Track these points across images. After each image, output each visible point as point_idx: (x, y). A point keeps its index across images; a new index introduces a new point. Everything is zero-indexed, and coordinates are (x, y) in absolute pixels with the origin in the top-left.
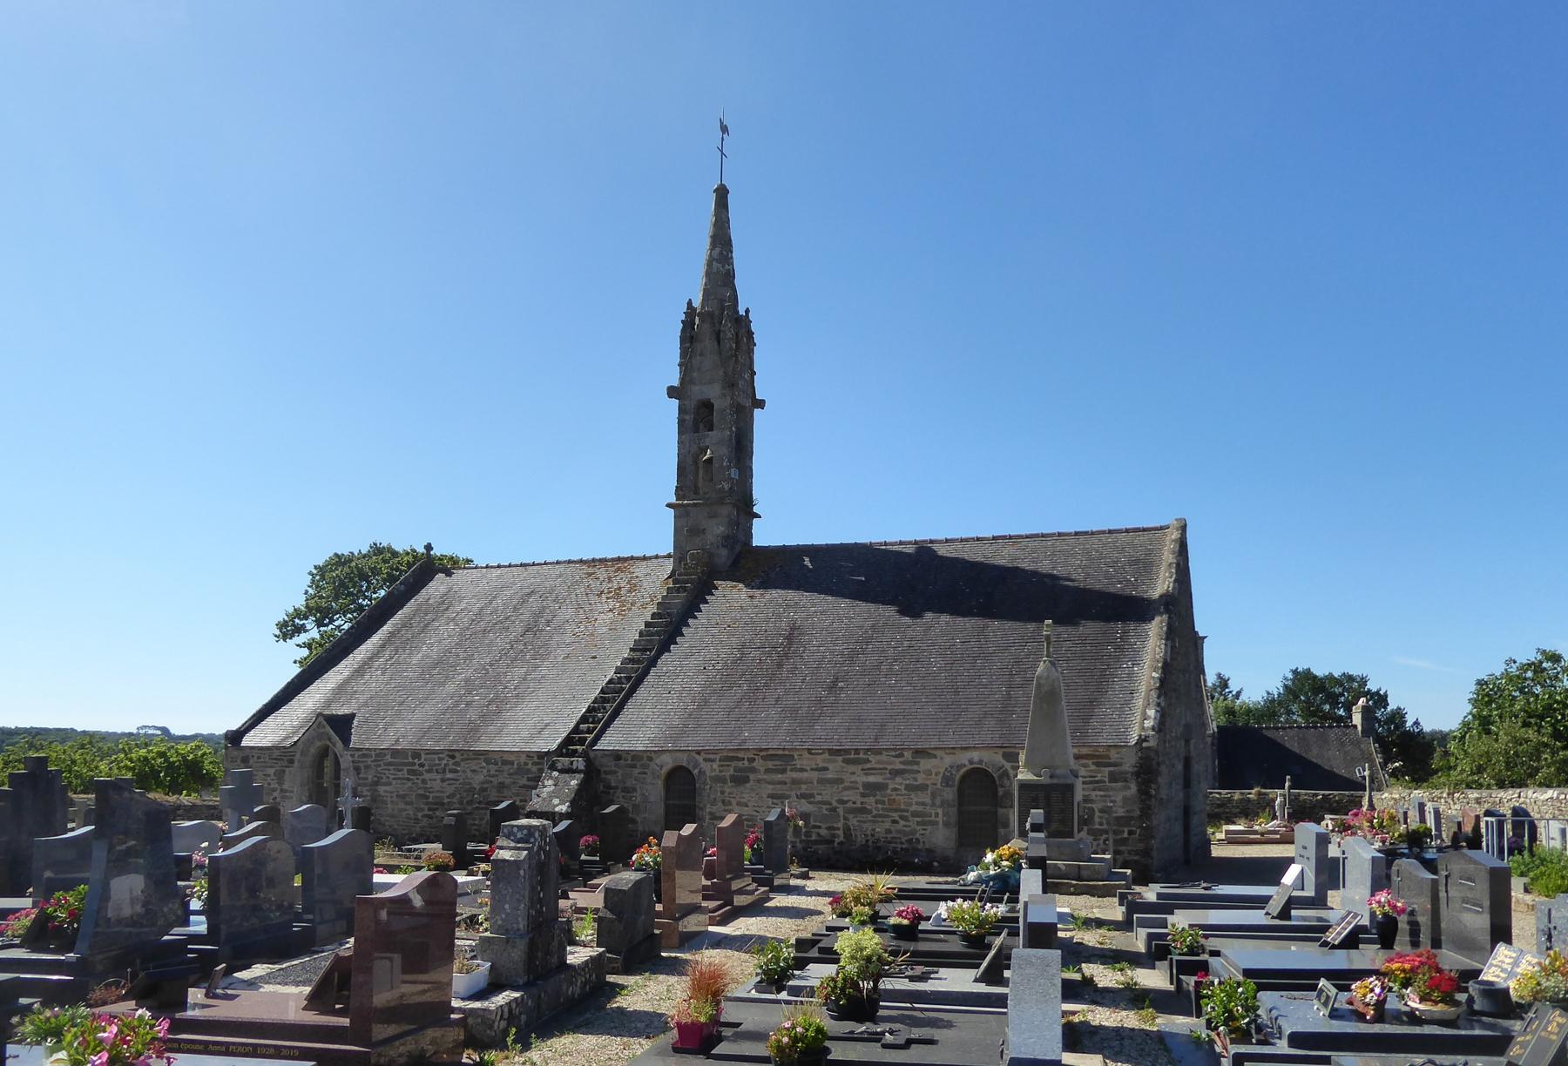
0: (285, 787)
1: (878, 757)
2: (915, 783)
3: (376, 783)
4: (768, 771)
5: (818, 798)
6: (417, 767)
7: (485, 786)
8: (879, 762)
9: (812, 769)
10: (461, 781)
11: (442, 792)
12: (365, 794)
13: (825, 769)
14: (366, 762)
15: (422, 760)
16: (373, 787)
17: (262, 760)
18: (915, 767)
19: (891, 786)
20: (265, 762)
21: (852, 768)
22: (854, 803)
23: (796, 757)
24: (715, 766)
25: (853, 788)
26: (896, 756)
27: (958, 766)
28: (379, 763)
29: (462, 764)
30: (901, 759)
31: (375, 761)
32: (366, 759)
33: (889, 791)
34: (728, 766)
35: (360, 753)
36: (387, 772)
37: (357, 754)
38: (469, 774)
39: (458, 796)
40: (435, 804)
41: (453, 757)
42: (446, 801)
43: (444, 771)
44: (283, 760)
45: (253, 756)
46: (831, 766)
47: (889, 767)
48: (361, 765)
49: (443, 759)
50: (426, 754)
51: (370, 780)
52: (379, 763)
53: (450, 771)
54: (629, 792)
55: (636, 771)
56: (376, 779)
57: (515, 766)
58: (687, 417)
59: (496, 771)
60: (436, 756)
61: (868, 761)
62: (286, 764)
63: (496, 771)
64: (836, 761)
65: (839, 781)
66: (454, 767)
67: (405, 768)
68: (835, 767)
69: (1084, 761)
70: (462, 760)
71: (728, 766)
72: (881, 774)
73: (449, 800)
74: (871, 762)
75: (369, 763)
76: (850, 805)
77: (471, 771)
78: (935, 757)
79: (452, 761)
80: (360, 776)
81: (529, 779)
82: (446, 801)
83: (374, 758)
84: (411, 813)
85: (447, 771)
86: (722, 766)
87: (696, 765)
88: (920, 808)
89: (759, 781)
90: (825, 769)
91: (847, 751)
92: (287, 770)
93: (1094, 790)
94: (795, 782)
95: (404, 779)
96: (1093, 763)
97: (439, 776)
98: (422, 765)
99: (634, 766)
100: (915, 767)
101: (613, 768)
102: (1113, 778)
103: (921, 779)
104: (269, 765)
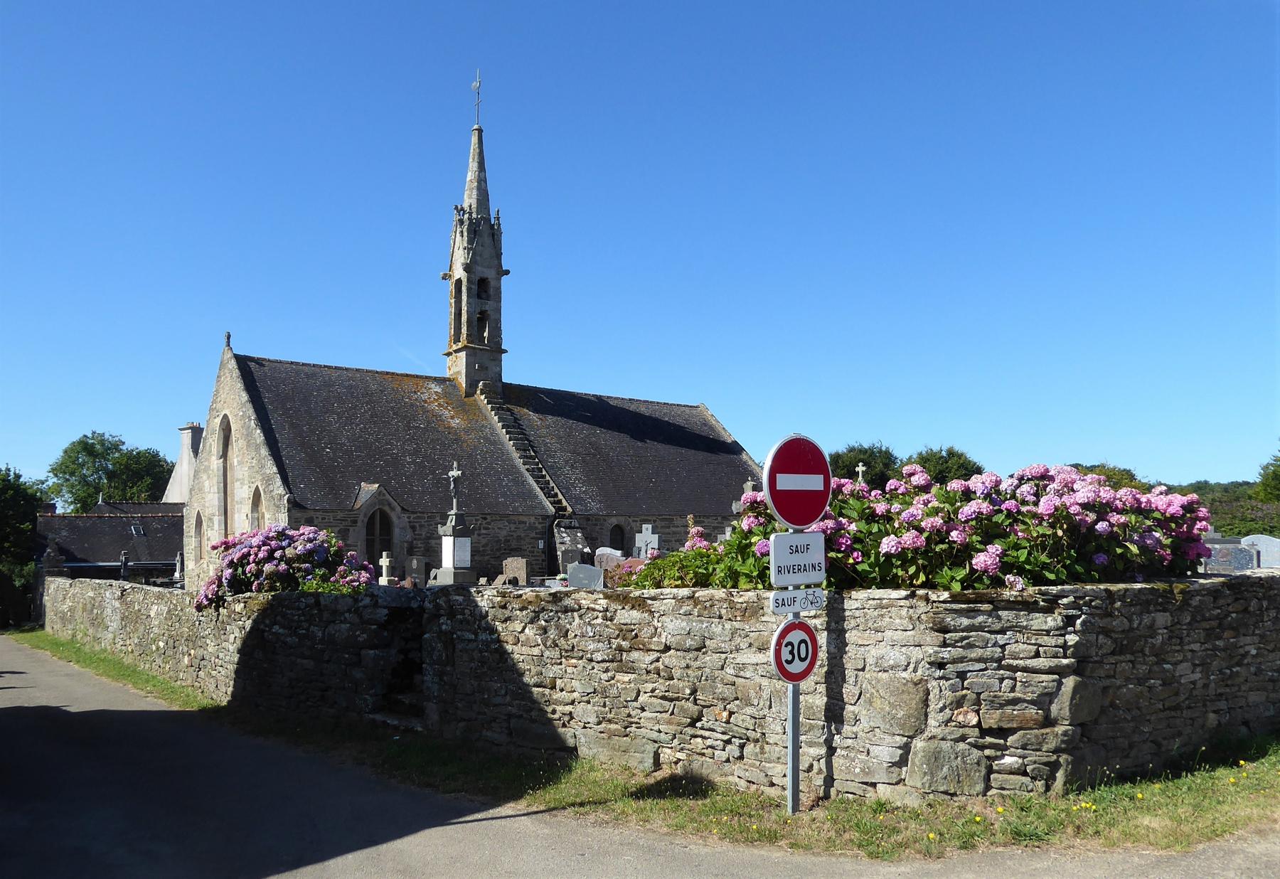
0: (349, 542)
3: (429, 538)
4: (662, 527)
7: (508, 538)
8: (708, 523)
11: (479, 543)
12: (420, 545)
17: (326, 520)
19: (713, 535)
20: (329, 522)
26: (715, 520)
29: (492, 523)
31: (427, 521)
37: (412, 516)
38: (497, 531)
39: (490, 545)
41: (485, 519)
42: (481, 549)
44: (347, 520)
45: (317, 518)
48: (417, 525)
51: (424, 536)
55: (598, 527)
56: (429, 535)
57: (527, 524)
58: (473, 287)
59: (516, 528)
61: (704, 522)
62: (350, 524)
63: (516, 528)
66: (486, 526)
70: (492, 521)
75: (423, 523)
77: (498, 528)
80: (416, 533)
81: (536, 534)
82: (481, 549)
87: (629, 524)
92: (351, 529)
94: (674, 533)
104: (334, 525)
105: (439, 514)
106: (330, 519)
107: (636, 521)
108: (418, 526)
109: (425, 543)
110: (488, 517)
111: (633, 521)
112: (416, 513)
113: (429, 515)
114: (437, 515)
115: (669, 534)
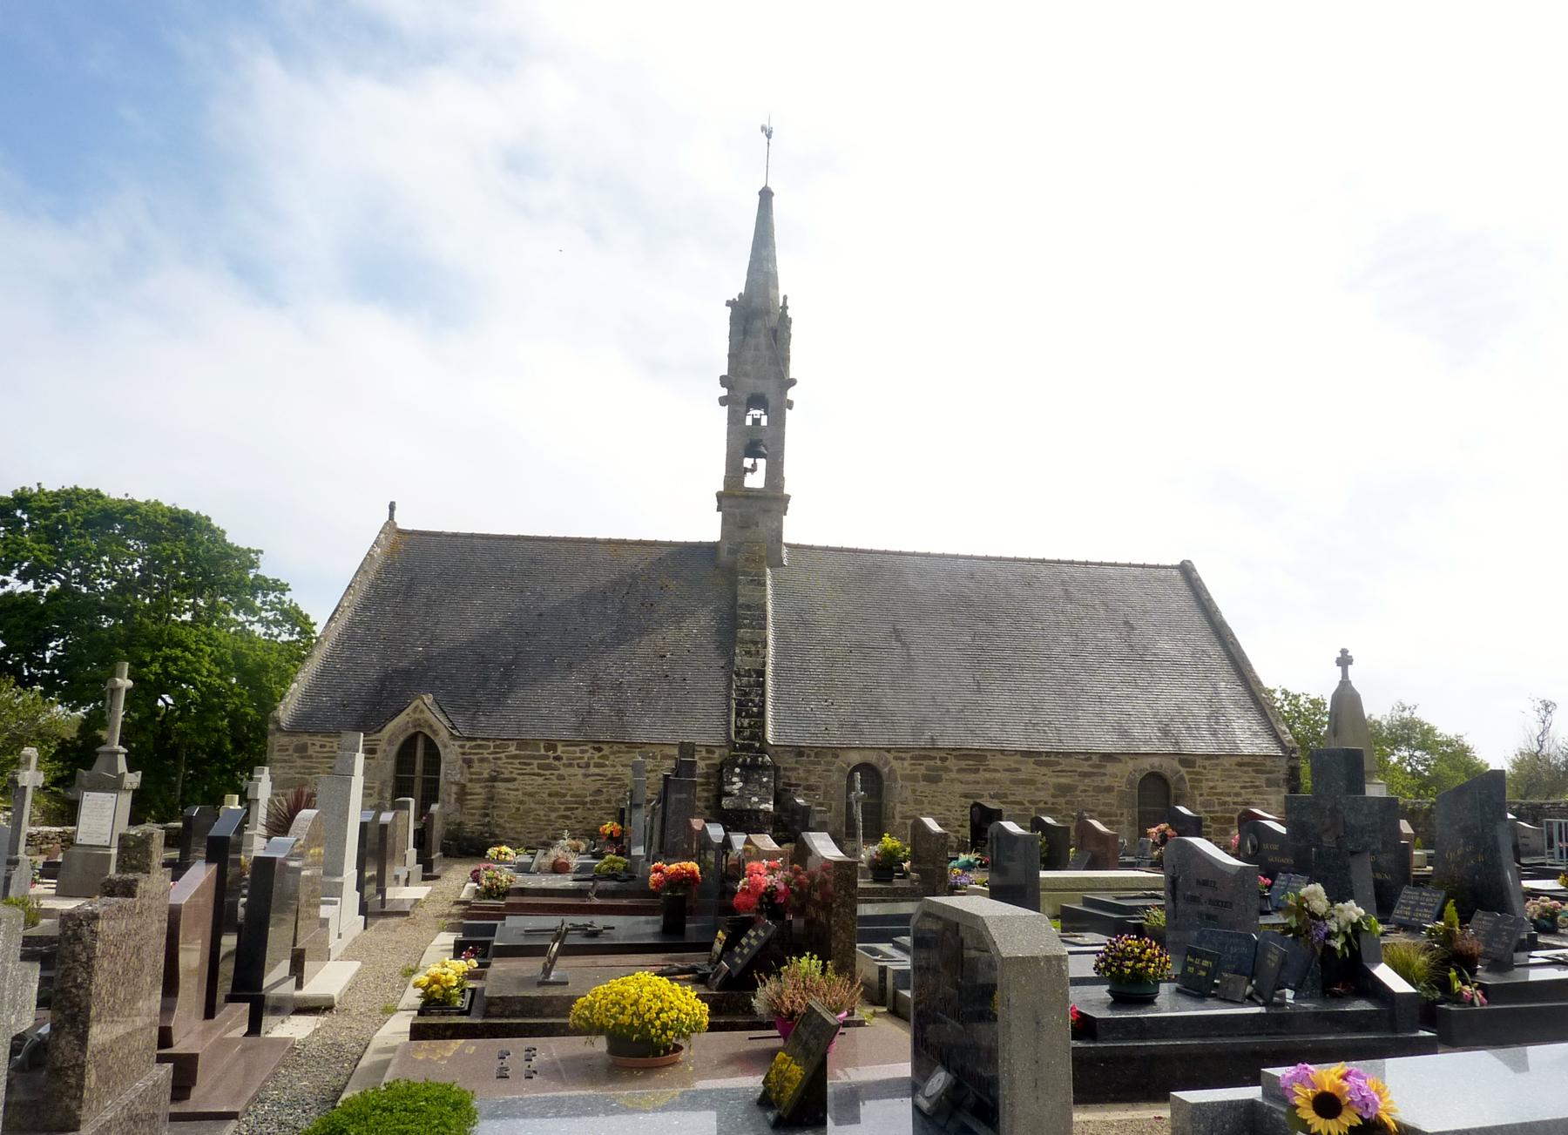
1: (1068, 760)
2: (1103, 785)
4: (960, 770)
5: (1011, 798)
6: (551, 761)
9: (1004, 770)
10: (610, 776)
13: (1018, 770)
14: (482, 754)
15: (559, 753)
16: (490, 784)
18: (1102, 771)
20: (331, 752)
21: (1044, 770)
22: (1045, 803)
23: (989, 757)
24: (906, 764)
25: (1043, 789)
26: (1086, 760)
27: (1141, 770)
28: (498, 756)
29: (612, 757)
30: (1090, 763)
32: (481, 751)
33: (1078, 793)
34: (920, 764)
35: (474, 743)
36: (509, 766)
37: (468, 744)
40: (576, 803)
41: (600, 750)
43: (588, 766)
45: (313, 744)
46: (1023, 768)
47: (1079, 770)
49: (587, 751)
50: (564, 746)
51: (486, 775)
52: (498, 756)
53: (597, 765)
54: (813, 790)
60: (577, 749)
61: (1059, 764)
64: (1027, 763)
65: (1032, 782)
66: (601, 761)
67: (536, 762)
68: (1028, 769)
69: (1246, 769)
70: (613, 753)
71: (920, 764)
72: (1071, 776)
73: (592, 798)
74: (1061, 764)
76: (1042, 805)
78: (1120, 761)
79: (597, 754)
80: (472, 770)
83: (492, 749)
84: (542, 813)
85: (592, 765)
86: (914, 764)
87: (887, 763)
88: (1106, 809)
89: (952, 780)
90: (1018, 770)
91: (1040, 753)
93: (1254, 794)
94: (988, 782)
95: (534, 774)
96: (1253, 770)
97: (583, 771)
98: (558, 758)
99: (819, 763)
100: (1102, 771)
101: (794, 765)
102: (1269, 783)
103: (1107, 781)
105: (515, 743)
106: (332, 747)
107: (903, 759)
108: (476, 761)
109: (487, 787)
110: (604, 746)
111: (896, 758)
112: (474, 739)
113: (498, 742)
114: (510, 742)
115: (978, 783)
